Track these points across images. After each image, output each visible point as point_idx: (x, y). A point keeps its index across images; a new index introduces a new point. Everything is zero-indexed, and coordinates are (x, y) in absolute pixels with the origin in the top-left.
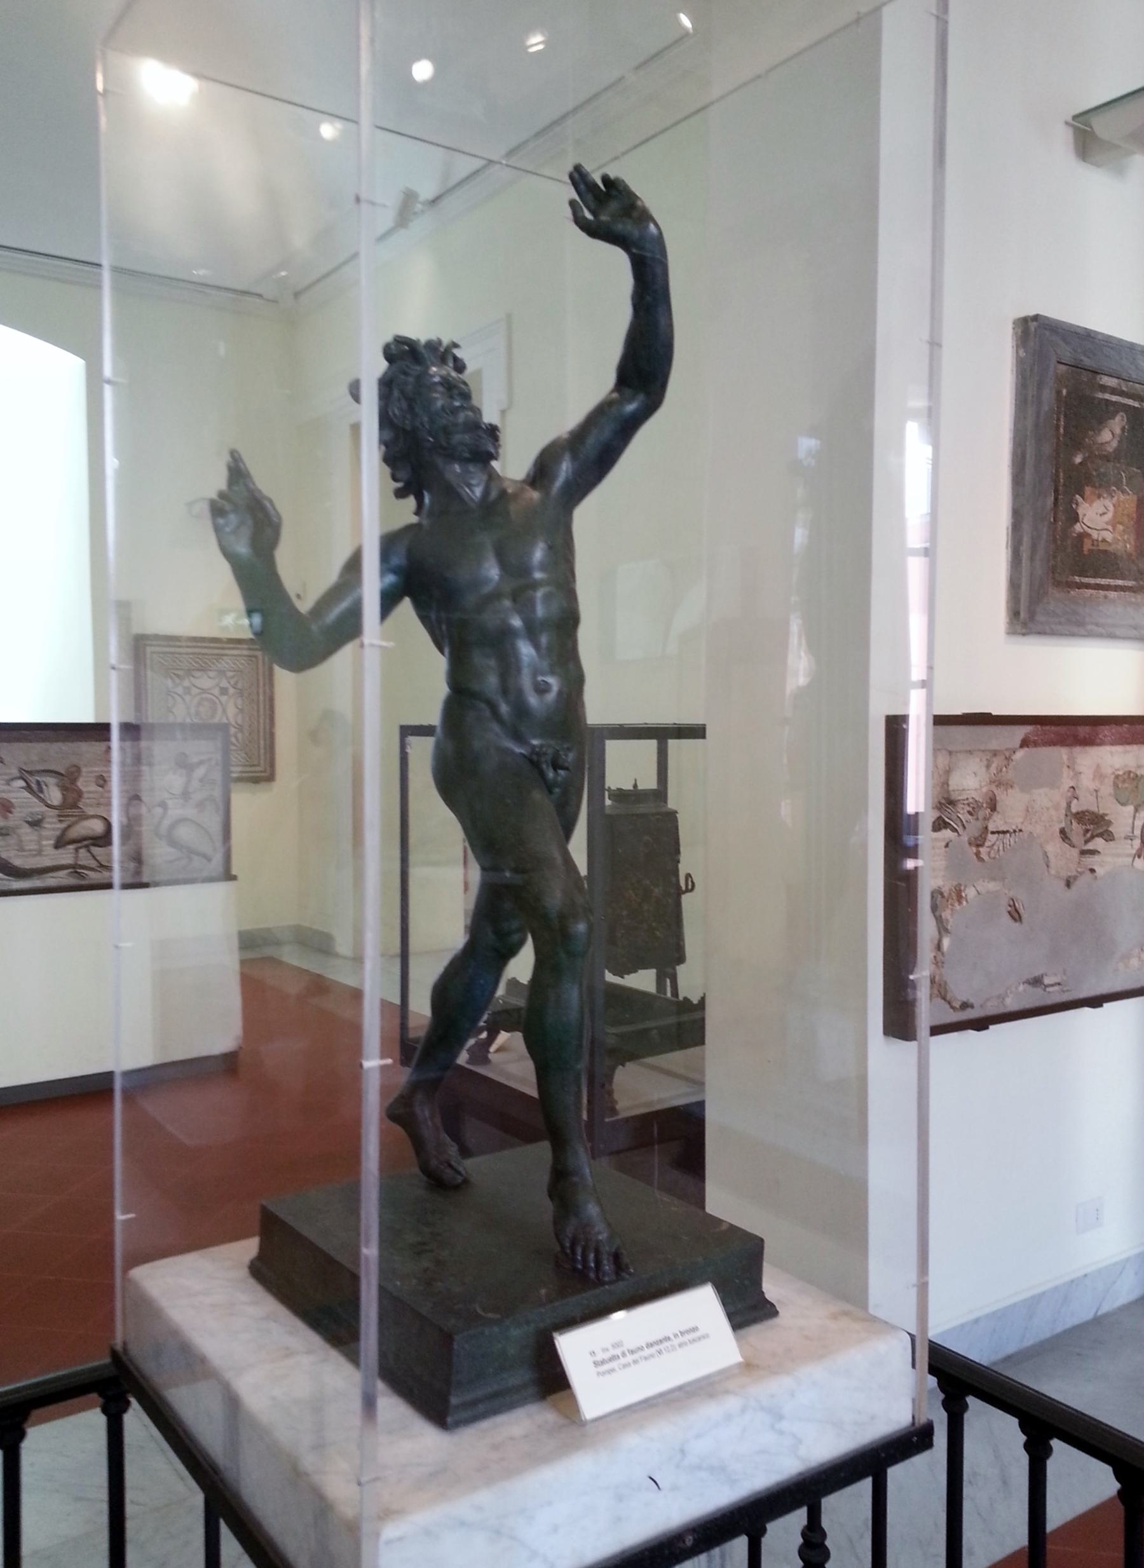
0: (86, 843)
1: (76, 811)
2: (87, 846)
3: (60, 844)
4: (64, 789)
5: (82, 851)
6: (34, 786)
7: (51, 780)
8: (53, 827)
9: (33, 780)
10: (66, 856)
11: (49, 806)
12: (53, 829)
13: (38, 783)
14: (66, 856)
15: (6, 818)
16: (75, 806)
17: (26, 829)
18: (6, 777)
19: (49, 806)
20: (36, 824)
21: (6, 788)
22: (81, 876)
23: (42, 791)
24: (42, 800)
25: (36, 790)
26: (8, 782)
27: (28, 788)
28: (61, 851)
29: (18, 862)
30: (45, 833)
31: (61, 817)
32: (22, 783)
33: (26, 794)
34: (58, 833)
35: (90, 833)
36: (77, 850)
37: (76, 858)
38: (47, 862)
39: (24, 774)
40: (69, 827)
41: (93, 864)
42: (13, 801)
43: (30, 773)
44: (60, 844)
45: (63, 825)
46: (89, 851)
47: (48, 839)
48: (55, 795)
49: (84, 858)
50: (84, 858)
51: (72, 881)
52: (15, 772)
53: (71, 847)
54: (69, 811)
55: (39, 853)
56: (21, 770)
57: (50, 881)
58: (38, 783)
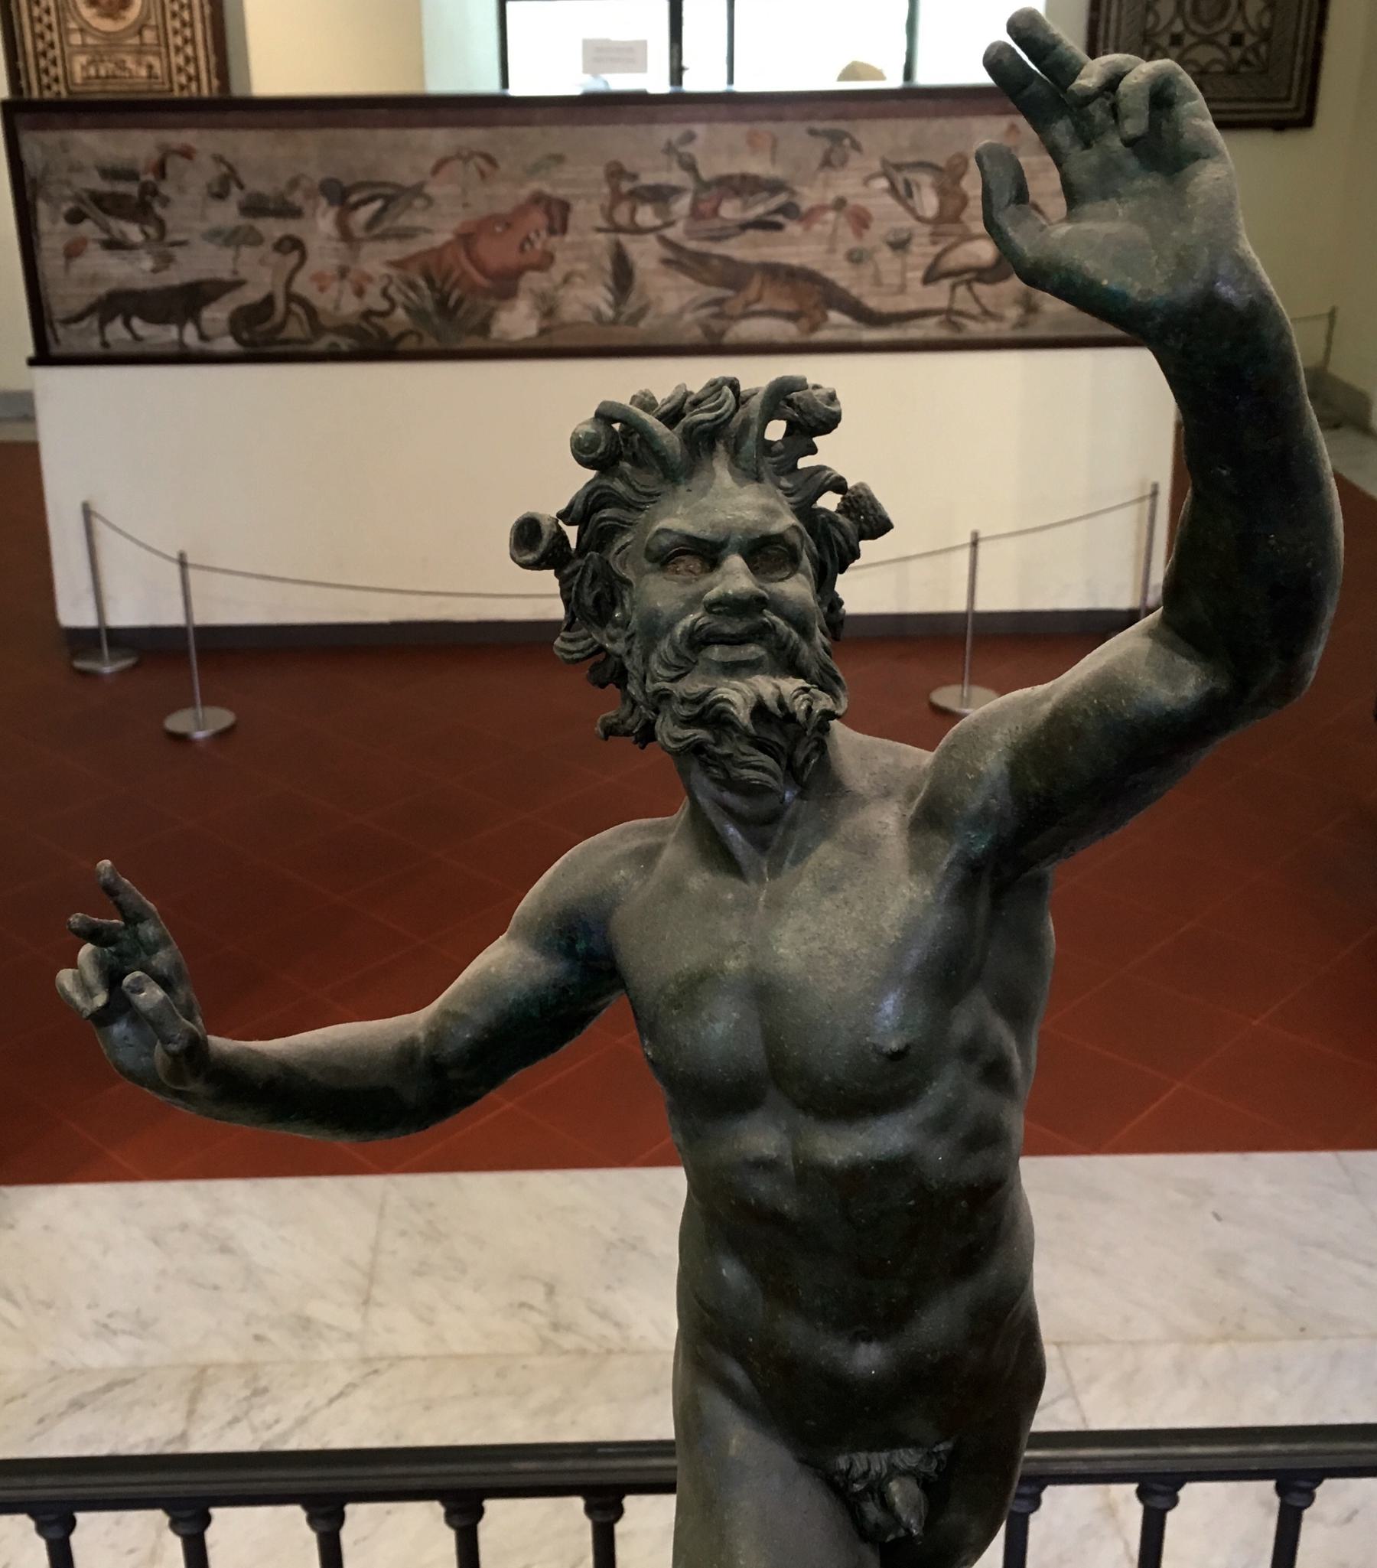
0: (967, 276)
1: (954, 228)
2: (969, 283)
3: (931, 276)
4: (942, 192)
5: (961, 290)
6: (901, 187)
7: (925, 179)
8: (923, 251)
9: (899, 179)
10: (938, 296)
11: (920, 219)
12: (924, 255)
13: (908, 185)
14: (938, 296)
15: (859, 235)
16: (956, 219)
17: (886, 253)
18: (866, 174)
19: (919, 219)
20: (900, 245)
21: (861, 189)
22: (957, 327)
23: (910, 195)
24: (912, 210)
25: (903, 194)
26: (866, 181)
27: (893, 190)
28: (931, 288)
29: (872, 302)
30: (911, 260)
31: (935, 237)
32: (883, 183)
33: (889, 200)
34: (929, 260)
35: (972, 262)
36: (953, 287)
37: (952, 298)
38: (910, 304)
39: (890, 169)
40: (945, 251)
41: (975, 309)
42: (873, 211)
43: (899, 167)
44: (931, 276)
45: (938, 249)
46: (970, 289)
47: (915, 268)
48: (929, 202)
49: (963, 299)
50: (963, 299)
51: (944, 334)
52: (877, 166)
53: (946, 283)
54: (946, 228)
55: (902, 289)
56: (884, 162)
57: (914, 332)
58: (908, 185)
